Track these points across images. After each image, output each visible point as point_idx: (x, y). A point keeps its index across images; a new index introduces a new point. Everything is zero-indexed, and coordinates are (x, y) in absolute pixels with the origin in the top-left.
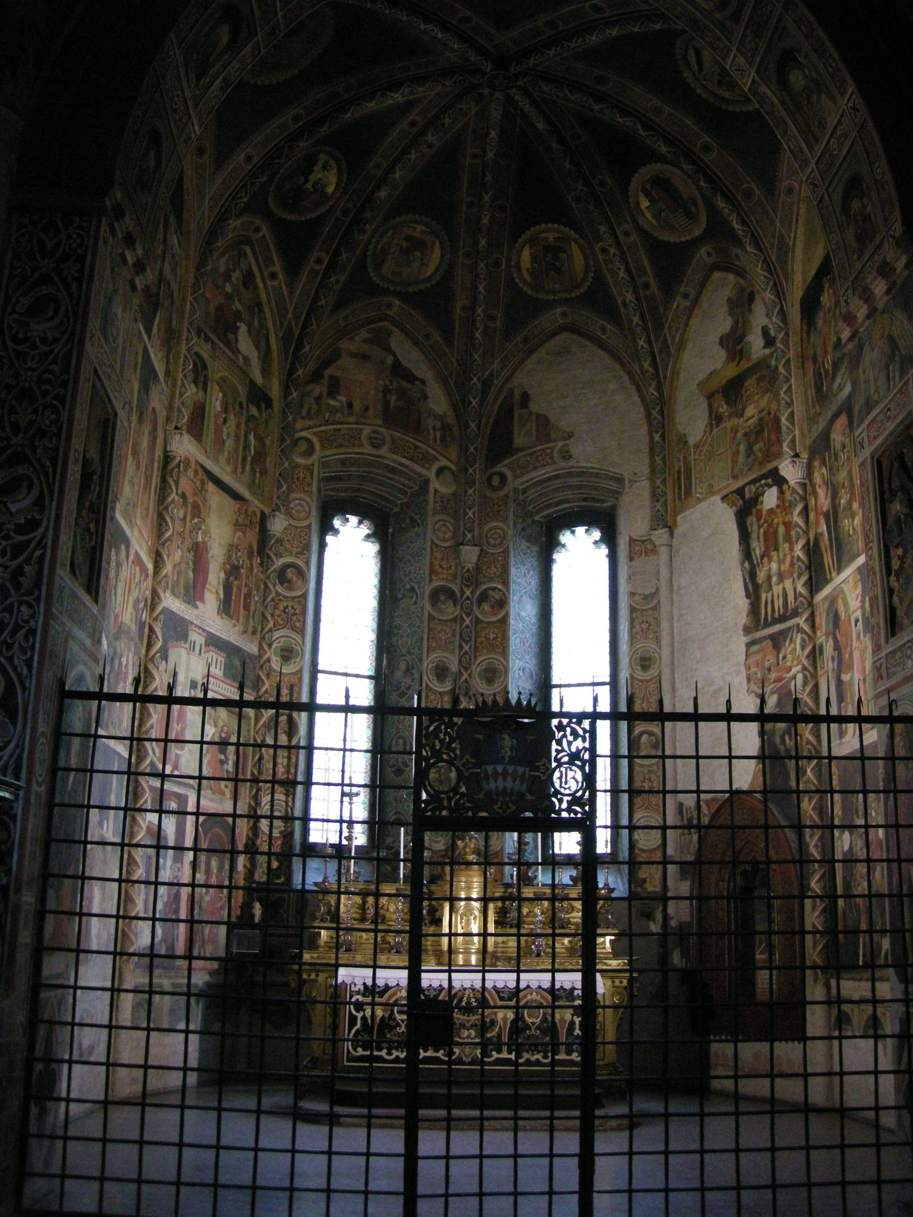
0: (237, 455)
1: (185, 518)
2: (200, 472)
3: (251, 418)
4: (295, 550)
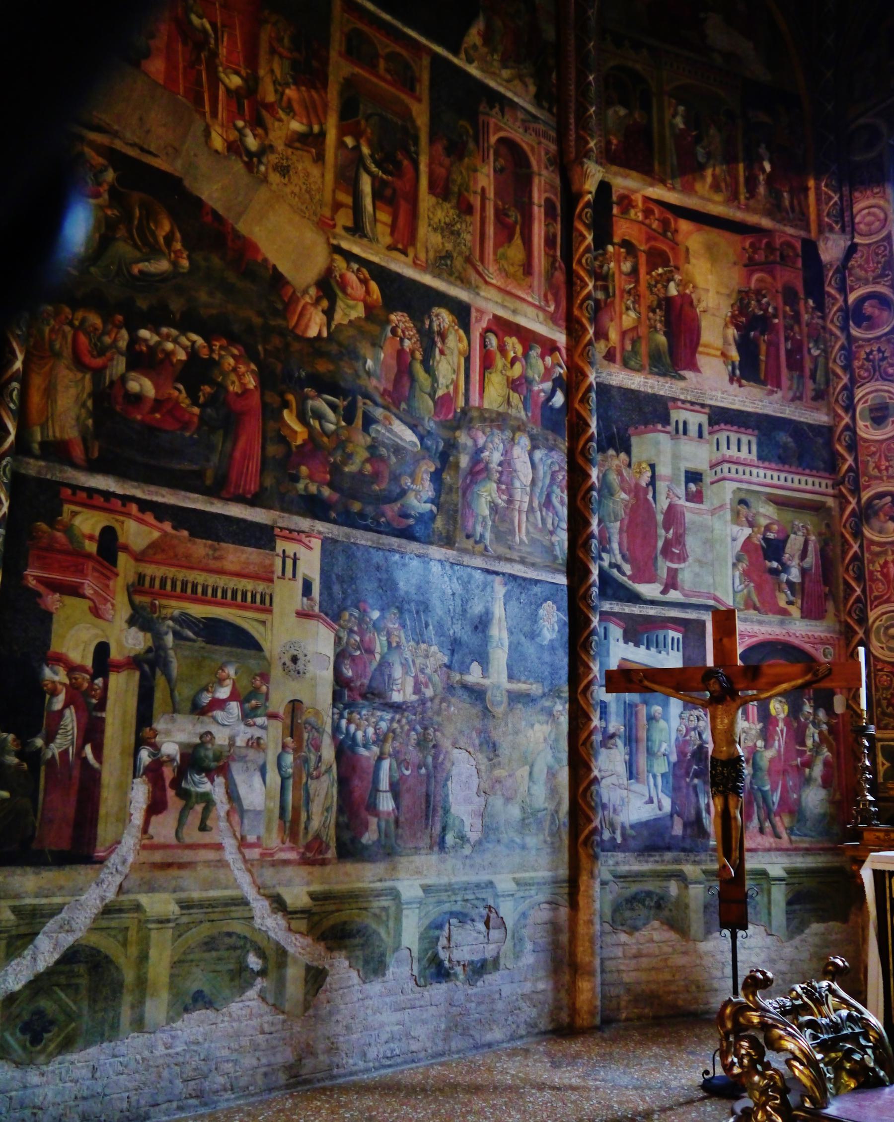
0: (735, 178)
1: (635, 271)
4: (870, 276)
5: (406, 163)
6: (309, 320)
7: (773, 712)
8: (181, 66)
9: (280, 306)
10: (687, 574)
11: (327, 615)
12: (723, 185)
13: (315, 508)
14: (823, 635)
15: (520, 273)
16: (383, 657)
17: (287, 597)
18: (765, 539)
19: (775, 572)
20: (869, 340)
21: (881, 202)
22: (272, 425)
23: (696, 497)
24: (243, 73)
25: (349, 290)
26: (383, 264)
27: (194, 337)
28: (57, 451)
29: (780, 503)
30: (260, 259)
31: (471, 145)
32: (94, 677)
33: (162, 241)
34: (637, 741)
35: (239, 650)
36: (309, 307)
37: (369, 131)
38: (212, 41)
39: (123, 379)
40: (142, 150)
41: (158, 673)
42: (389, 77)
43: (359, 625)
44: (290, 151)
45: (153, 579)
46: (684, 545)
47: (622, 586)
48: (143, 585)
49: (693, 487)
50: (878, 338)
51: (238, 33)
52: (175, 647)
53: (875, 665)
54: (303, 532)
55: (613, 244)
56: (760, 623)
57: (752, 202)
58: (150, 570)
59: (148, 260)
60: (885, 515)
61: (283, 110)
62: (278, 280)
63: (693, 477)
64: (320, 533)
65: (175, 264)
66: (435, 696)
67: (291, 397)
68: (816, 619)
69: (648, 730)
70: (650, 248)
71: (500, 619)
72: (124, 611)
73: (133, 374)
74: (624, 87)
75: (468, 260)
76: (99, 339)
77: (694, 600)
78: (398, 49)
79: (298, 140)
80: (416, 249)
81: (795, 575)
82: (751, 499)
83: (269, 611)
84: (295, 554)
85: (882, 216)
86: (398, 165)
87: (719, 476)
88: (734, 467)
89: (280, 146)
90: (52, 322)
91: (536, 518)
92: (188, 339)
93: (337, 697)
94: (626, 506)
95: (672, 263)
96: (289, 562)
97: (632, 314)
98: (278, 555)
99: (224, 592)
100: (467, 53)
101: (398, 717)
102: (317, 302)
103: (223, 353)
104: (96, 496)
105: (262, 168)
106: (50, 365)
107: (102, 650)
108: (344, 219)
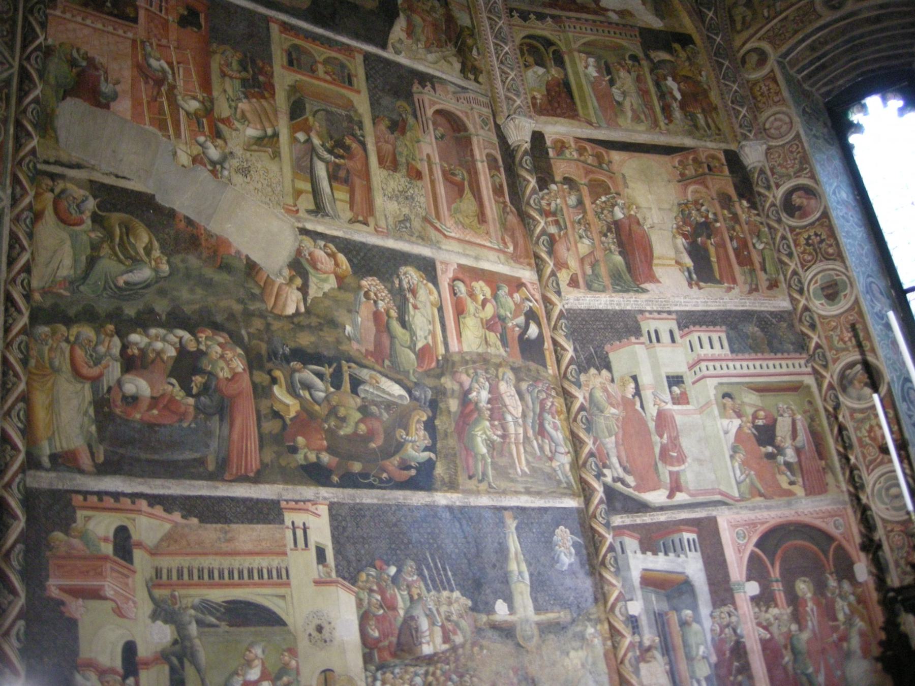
0: (652, 109)
1: (580, 202)
2: (588, 146)
3: (655, 67)
4: (791, 171)
5: (354, 145)
6: (287, 298)
7: (800, 594)
8: (145, 101)
9: (257, 291)
10: (690, 474)
11: (344, 578)
12: (643, 117)
13: (316, 474)
14: (830, 508)
15: (475, 222)
16: (407, 612)
17: (302, 566)
18: (757, 427)
19: (771, 456)
20: (805, 227)
21: (784, 109)
22: (265, 404)
23: (681, 400)
24: (200, 97)
25: (319, 266)
26: (347, 236)
27: (181, 333)
28: (64, 461)
29: (761, 390)
30: (233, 252)
31: (411, 120)
32: (125, 677)
33: (142, 251)
34: (674, 650)
35: (263, 629)
36: (284, 287)
37: (317, 124)
38: (170, 77)
39: (119, 383)
40: (117, 176)
41: (187, 664)
42: (328, 78)
43: (378, 584)
44: (248, 154)
45: (169, 571)
46: (680, 447)
47: (627, 498)
48: (161, 578)
49: (676, 390)
50: (812, 224)
51: (191, 66)
52: (200, 635)
53: (885, 527)
54: (309, 501)
55: (554, 182)
56: (768, 508)
57: (671, 126)
58: (165, 562)
59: (131, 271)
60: (860, 382)
61: (238, 121)
62: (252, 268)
63: (675, 380)
64: (325, 498)
65: (156, 270)
66: (466, 641)
67: (278, 373)
68: (820, 493)
69: (683, 636)
70: (590, 181)
71: (516, 554)
72: (147, 607)
73: (128, 377)
74: (537, 51)
75: (426, 219)
76: (94, 349)
77: (701, 499)
78: (334, 54)
79: (255, 144)
80: (375, 218)
81: (790, 455)
82: (735, 394)
83: (288, 585)
84: (304, 524)
85: (787, 120)
86: (347, 148)
87: (699, 375)
88: (711, 364)
89: (238, 151)
90: (50, 341)
91: (533, 448)
92: (176, 337)
93: (367, 659)
94: (617, 420)
95: (612, 191)
96: (300, 533)
97: (586, 241)
98: (288, 528)
99: (241, 573)
100: (394, 47)
101: (431, 669)
102: (291, 280)
103: (209, 343)
104: (105, 498)
105: (226, 173)
106: (52, 381)
107: (130, 649)
108: (306, 202)
